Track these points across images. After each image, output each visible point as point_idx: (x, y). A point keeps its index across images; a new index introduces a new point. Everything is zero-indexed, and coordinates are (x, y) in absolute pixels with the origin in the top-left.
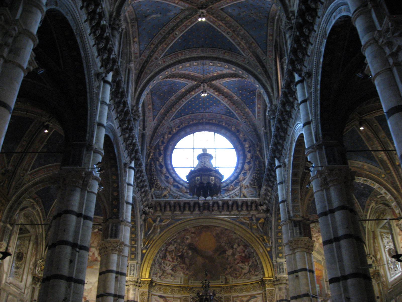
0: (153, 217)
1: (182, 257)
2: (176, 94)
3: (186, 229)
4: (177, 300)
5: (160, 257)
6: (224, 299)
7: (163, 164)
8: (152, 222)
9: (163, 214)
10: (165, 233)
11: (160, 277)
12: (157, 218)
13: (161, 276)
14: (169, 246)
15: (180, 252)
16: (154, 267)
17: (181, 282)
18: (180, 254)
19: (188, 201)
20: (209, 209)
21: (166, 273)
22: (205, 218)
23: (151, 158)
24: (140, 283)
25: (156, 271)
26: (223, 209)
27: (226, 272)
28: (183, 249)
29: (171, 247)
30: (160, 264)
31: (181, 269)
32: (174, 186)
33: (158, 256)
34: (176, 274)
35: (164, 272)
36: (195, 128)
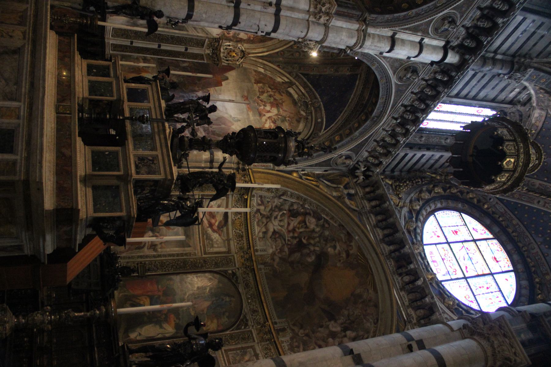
0: (351, 184)
1: (300, 246)
2: (545, 184)
3: (353, 235)
4: (225, 247)
5: (292, 204)
6: (244, 330)
7: (433, 194)
8: (344, 185)
9: (362, 198)
10: (335, 203)
11: (258, 211)
12: (353, 189)
13: (261, 214)
14: (314, 217)
15: (307, 240)
16: (273, 195)
17: (257, 250)
18: (304, 241)
19: (399, 228)
20: (399, 267)
21: (267, 223)
22: (382, 264)
23: (432, 177)
24: (244, 170)
25: (268, 202)
26: (409, 292)
27: (296, 329)
28: (314, 245)
29: (313, 220)
30: (279, 208)
31: (278, 248)
32: (410, 212)
33: (294, 201)
34: (270, 240)
35: (269, 218)
36: (504, 238)
